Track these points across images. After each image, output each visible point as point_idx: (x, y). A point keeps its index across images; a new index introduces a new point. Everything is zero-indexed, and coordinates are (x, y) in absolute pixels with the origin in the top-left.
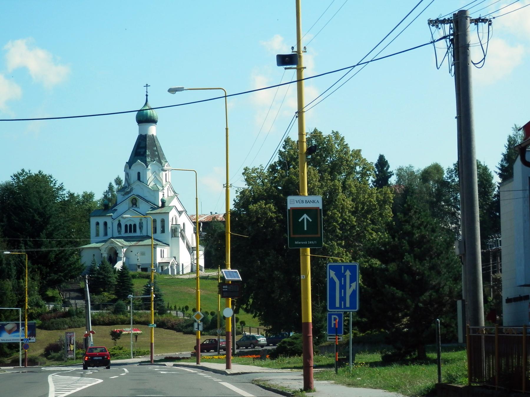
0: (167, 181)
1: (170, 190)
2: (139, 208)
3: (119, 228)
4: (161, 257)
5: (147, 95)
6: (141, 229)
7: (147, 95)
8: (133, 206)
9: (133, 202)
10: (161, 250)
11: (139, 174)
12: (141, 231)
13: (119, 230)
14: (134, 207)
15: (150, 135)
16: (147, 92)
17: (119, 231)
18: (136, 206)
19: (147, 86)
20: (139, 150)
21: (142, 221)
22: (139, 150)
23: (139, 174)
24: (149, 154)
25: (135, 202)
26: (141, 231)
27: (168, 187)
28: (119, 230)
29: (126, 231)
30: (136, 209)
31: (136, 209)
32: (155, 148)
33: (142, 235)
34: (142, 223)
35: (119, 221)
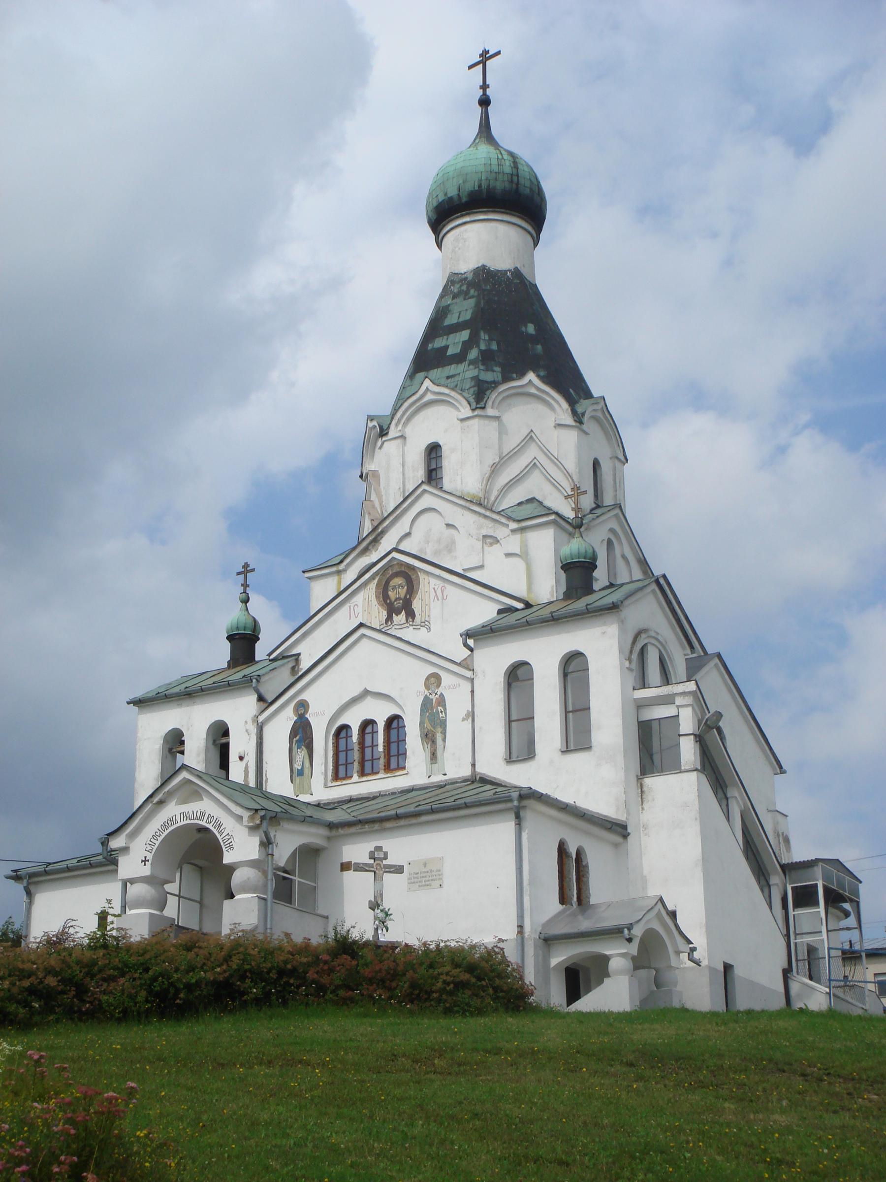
0: (608, 500)
1: (624, 557)
2: (426, 624)
3: (301, 755)
4: (563, 899)
5: (485, 102)
6: (434, 742)
7: (485, 102)
8: (389, 619)
9: (392, 595)
10: (562, 850)
11: (434, 451)
12: (434, 757)
13: (297, 766)
14: (401, 627)
15: (506, 271)
16: (484, 86)
17: (301, 773)
18: (411, 614)
19: (485, 57)
20: (439, 343)
21: (440, 691)
22: (439, 343)
23: (434, 451)
24: (494, 347)
25: (403, 592)
26: (434, 757)
27: (612, 530)
28: (297, 766)
29: (339, 774)
30: (408, 634)
31: (408, 634)
32: (531, 329)
33: (437, 778)
34: (442, 701)
35: (303, 706)
